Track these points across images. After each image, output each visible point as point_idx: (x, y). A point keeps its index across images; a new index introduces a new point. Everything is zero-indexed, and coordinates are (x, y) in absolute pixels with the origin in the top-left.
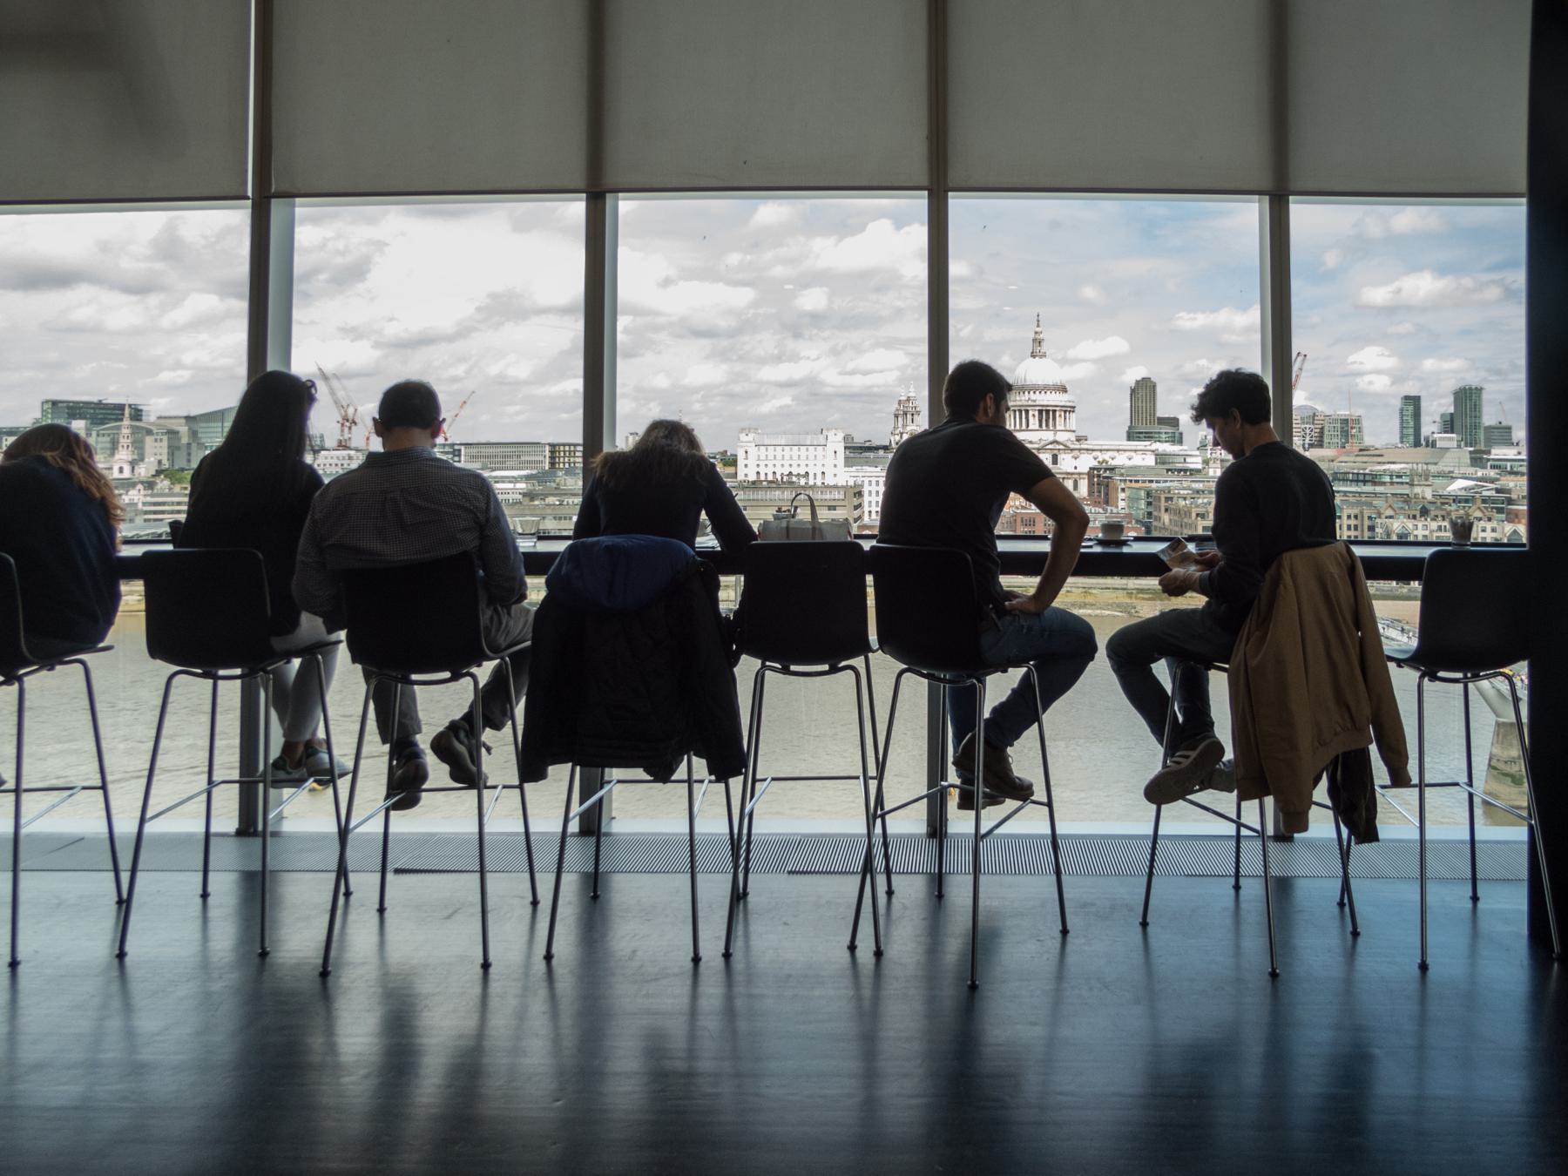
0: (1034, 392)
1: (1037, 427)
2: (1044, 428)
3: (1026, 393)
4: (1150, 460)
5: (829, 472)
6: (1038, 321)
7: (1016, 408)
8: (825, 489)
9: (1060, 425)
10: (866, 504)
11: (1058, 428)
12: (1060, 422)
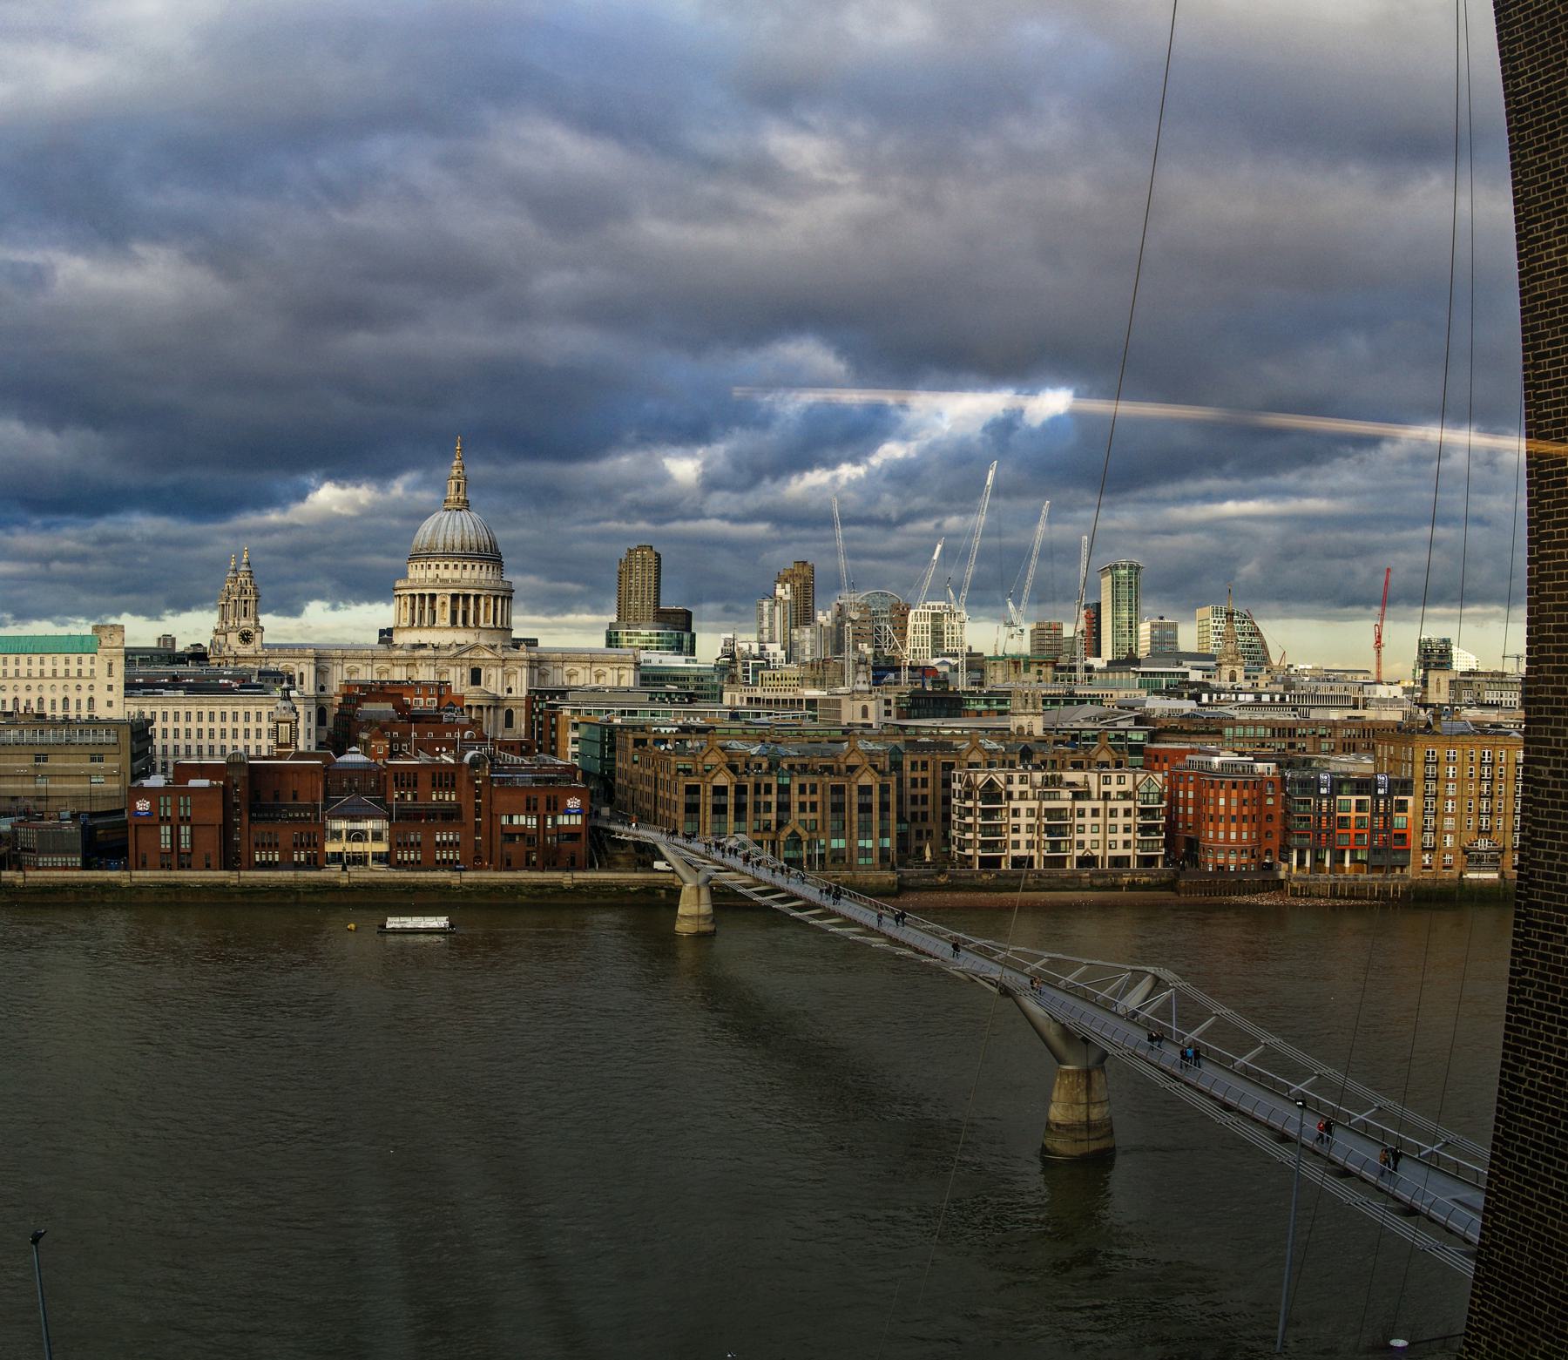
0: (446, 567)
1: (447, 623)
3: (433, 566)
4: (629, 678)
5: (101, 696)
7: (416, 592)
8: (85, 728)
10: (159, 750)
11: (482, 624)
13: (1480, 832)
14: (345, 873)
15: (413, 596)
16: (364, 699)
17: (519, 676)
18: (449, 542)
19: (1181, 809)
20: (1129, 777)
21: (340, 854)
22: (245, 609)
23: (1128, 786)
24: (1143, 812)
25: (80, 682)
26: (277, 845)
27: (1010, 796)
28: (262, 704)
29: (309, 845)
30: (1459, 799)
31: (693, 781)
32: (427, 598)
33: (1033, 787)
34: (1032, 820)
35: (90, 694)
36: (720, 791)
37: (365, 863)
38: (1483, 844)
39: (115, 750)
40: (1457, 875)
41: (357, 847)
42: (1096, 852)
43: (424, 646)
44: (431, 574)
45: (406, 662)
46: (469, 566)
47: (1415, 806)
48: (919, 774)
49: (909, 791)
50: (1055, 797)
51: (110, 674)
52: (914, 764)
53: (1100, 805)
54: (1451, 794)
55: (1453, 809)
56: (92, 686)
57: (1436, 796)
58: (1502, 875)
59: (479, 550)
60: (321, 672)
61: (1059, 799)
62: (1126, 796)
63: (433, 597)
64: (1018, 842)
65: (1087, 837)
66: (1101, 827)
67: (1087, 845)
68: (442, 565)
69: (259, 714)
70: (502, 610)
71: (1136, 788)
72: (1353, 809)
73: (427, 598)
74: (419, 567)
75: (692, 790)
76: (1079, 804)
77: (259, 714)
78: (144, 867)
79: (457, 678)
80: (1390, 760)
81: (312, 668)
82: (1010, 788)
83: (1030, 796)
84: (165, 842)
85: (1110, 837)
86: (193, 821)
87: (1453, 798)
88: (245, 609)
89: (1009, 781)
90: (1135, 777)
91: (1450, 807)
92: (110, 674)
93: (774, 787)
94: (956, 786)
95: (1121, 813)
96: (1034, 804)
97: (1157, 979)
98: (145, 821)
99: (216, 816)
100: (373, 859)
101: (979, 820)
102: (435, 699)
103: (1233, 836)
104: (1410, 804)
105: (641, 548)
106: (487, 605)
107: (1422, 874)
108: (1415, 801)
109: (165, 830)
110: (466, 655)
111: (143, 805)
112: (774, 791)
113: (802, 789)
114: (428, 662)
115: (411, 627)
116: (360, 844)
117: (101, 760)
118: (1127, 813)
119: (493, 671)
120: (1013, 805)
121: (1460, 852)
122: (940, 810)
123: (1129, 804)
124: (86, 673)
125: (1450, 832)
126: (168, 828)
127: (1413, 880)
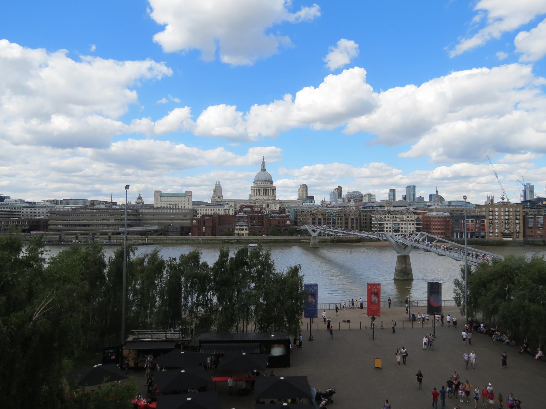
1: (262, 195)
6: (263, 158)
7: (255, 188)
11: (270, 195)
13: (506, 228)
15: (255, 189)
16: (244, 207)
20: (413, 216)
23: (413, 219)
27: (385, 220)
31: (313, 217)
33: (390, 218)
34: (390, 226)
35: (184, 205)
36: (320, 219)
37: (244, 235)
39: (189, 214)
41: (242, 232)
42: (405, 233)
43: (257, 199)
46: (266, 183)
48: (364, 217)
49: (362, 221)
50: (396, 221)
51: (189, 201)
52: (363, 215)
53: (406, 222)
54: (497, 219)
62: (412, 221)
63: (259, 189)
65: (404, 230)
66: (407, 228)
67: (404, 232)
69: (221, 210)
75: (314, 219)
76: (402, 222)
77: (221, 210)
79: (265, 205)
81: (234, 204)
82: (385, 219)
83: (390, 220)
89: (385, 217)
90: (415, 216)
92: (189, 201)
93: (332, 219)
94: (373, 219)
95: (411, 224)
96: (391, 222)
101: (378, 226)
106: (270, 191)
110: (266, 201)
112: (332, 220)
115: (255, 196)
117: (186, 216)
118: (413, 224)
119: (272, 204)
121: (500, 233)
123: (413, 222)
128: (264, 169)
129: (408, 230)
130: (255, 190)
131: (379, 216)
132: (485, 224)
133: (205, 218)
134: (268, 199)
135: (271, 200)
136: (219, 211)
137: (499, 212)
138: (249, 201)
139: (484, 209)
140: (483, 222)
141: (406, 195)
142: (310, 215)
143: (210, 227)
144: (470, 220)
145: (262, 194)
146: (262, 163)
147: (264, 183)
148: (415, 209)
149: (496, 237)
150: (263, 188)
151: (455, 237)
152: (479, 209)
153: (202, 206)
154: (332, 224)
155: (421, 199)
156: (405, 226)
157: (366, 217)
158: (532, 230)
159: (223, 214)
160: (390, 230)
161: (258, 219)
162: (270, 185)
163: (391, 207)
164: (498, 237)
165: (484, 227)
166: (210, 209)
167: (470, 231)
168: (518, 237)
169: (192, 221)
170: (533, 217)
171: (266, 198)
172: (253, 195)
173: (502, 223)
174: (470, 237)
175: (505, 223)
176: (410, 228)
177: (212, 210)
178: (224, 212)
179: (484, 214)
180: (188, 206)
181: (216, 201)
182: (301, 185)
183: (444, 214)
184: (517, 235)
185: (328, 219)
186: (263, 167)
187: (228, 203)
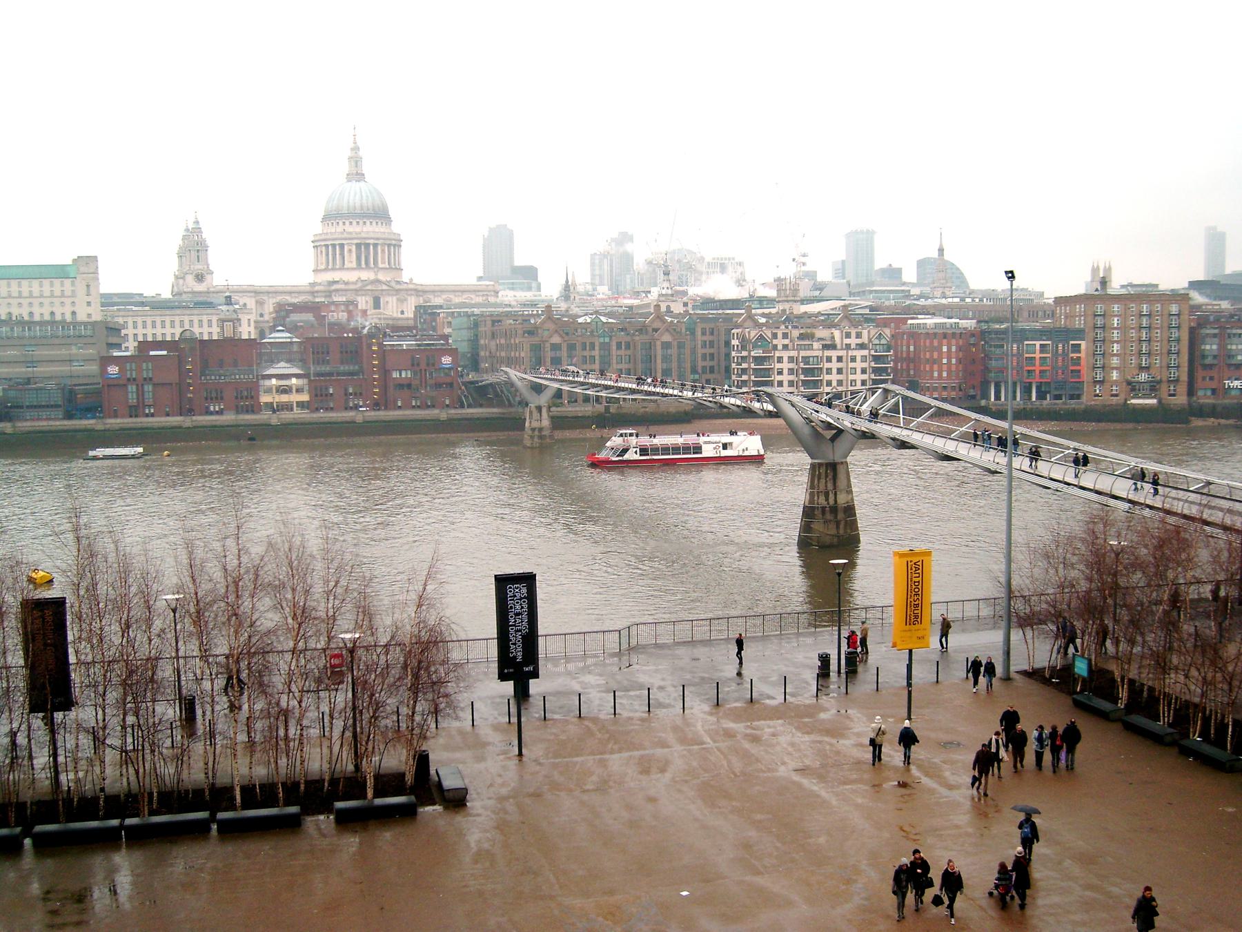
0: (351, 223)
1: (354, 265)
2: (363, 265)
3: (341, 223)
9: (383, 262)
11: (381, 265)
12: (383, 259)
13: (1141, 368)
14: (275, 415)
15: (327, 246)
16: (291, 311)
17: (409, 302)
18: (351, 204)
19: (904, 348)
20: (865, 333)
21: (272, 403)
22: (198, 257)
23: (865, 339)
24: (876, 359)
25: (63, 299)
26: (222, 398)
27: (775, 348)
28: (212, 314)
29: (247, 398)
30: (1123, 344)
31: (535, 340)
32: (337, 247)
35: (72, 309)
36: (555, 347)
38: (1143, 377)
40: (1123, 401)
41: (284, 398)
42: (840, 389)
43: (337, 282)
44: (340, 229)
45: (323, 294)
46: (368, 223)
47: (1087, 348)
49: (700, 351)
50: (810, 347)
52: (704, 334)
54: (1116, 339)
55: (1117, 351)
56: (73, 302)
57: (1104, 341)
58: (1160, 402)
59: (373, 210)
60: (260, 303)
61: (812, 349)
62: (862, 346)
64: (782, 381)
65: (834, 377)
66: (844, 371)
67: (834, 383)
68: (347, 223)
70: (394, 254)
71: (870, 340)
72: (1038, 352)
73: (337, 247)
74: (330, 224)
76: (827, 353)
78: (116, 416)
79: (363, 302)
80: (1066, 317)
81: (253, 300)
82: (775, 342)
84: (132, 399)
85: (851, 377)
86: (156, 380)
87: (1117, 342)
88: (198, 257)
89: (775, 336)
91: (1115, 349)
93: (597, 344)
94: (735, 342)
97: (886, 391)
98: (116, 383)
99: (173, 377)
100: (297, 406)
101: (753, 366)
102: (345, 314)
103: (945, 374)
104: (1083, 347)
105: (498, 227)
106: (383, 251)
107: (1094, 400)
108: (1087, 344)
109: (132, 388)
111: (113, 370)
113: (619, 346)
114: (340, 293)
115: (326, 270)
116: (286, 396)
119: (389, 299)
120: (777, 354)
121: (1124, 383)
122: (723, 364)
123: (865, 352)
124: (68, 293)
125: (1116, 368)
126: (134, 388)
127: (1086, 406)
128: (357, 175)
129: (847, 378)
130: (329, 250)
131: (754, 334)
132: (1083, 355)
133: (152, 353)
134: (378, 281)
135: (387, 283)
136: (201, 326)
137: (1123, 316)
138: (308, 289)
139: (1080, 308)
140: (1077, 348)
141: (843, 262)
142: (520, 332)
143: (171, 384)
144: (1038, 343)
145: (351, 262)
146: (352, 149)
147: (361, 222)
148: (872, 309)
149: (1112, 395)
150: (356, 241)
151: (993, 399)
152: (1065, 306)
153: (140, 308)
154: (597, 362)
155: (893, 273)
156: (840, 365)
157: (711, 338)
158: (1214, 373)
159: (215, 337)
160: (792, 378)
161: (342, 352)
162: (382, 230)
163: (795, 301)
164: (1116, 395)
165: (1079, 364)
166: (168, 320)
167: (1038, 379)
168: (1174, 395)
169: (103, 371)
170: (1216, 331)
171: (366, 275)
172: (323, 267)
173: (1132, 351)
174: (1037, 399)
175: (1140, 353)
176: (853, 371)
177: (177, 324)
178: (219, 330)
179: (1080, 324)
180: (89, 310)
181: (189, 290)
182: (491, 230)
183: (960, 326)
184: (1172, 388)
185: (584, 345)
186: (353, 163)
187: (230, 297)
